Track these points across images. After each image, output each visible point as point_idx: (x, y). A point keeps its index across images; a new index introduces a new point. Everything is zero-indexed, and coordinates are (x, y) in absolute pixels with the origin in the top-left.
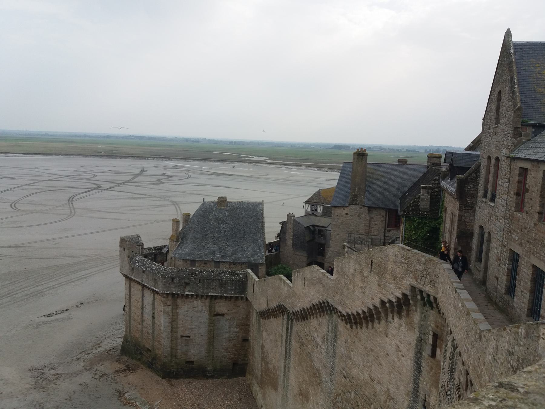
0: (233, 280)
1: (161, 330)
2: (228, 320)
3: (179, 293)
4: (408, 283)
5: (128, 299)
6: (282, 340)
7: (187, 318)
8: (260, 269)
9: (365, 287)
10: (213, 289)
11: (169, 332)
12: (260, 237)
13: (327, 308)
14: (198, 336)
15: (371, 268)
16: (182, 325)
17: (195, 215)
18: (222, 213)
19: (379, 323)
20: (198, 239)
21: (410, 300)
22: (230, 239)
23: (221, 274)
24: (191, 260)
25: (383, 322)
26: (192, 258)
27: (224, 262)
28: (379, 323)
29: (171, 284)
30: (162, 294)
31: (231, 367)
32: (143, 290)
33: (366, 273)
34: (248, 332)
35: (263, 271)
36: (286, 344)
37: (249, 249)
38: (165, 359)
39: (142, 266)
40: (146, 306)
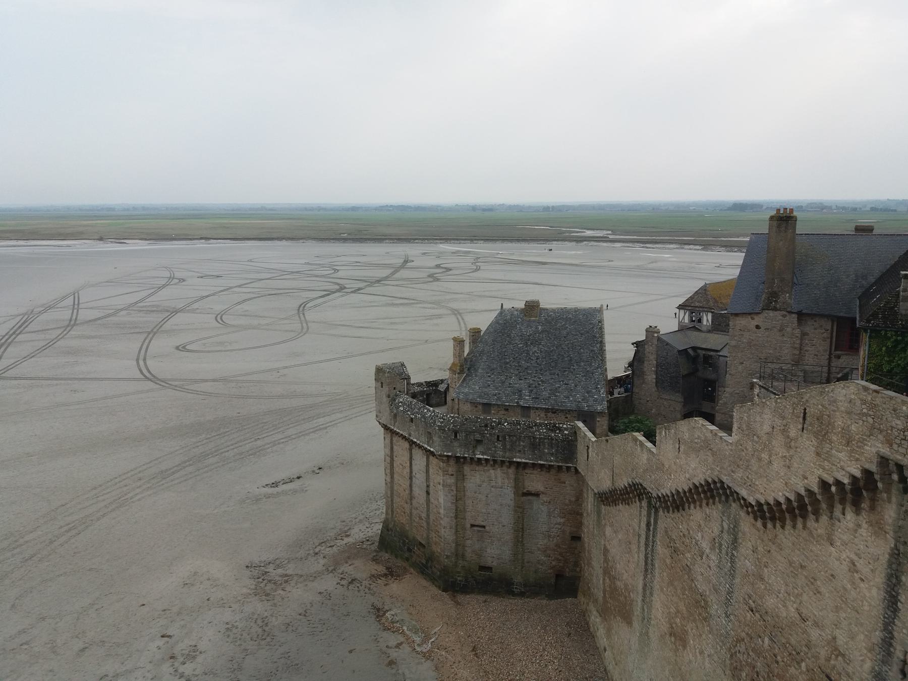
0: (552, 439)
1: (439, 513)
2: (547, 504)
3: (466, 455)
4: (874, 450)
5: (389, 462)
6: (639, 542)
7: (480, 496)
8: (598, 421)
9: (791, 457)
10: (520, 451)
11: (452, 517)
12: (597, 368)
13: (721, 492)
14: (497, 527)
15: (804, 423)
16: (473, 507)
17: (488, 331)
18: (531, 327)
19: (817, 520)
20: (493, 369)
21: (876, 481)
22: (546, 371)
23: (532, 428)
24: (484, 404)
25: (824, 519)
26: (485, 401)
27: (537, 409)
28: (817, 520)
29: (453, 441)
30: (440, 456)
31: (553, 581)
32: (411, 450)
33: (793, 433)
34: (580, 525)
35: (603, 425)
36: (646, 550)
37: (579, 388)
38: (446, 560)
39: (409, 411)
40: (416, 474)
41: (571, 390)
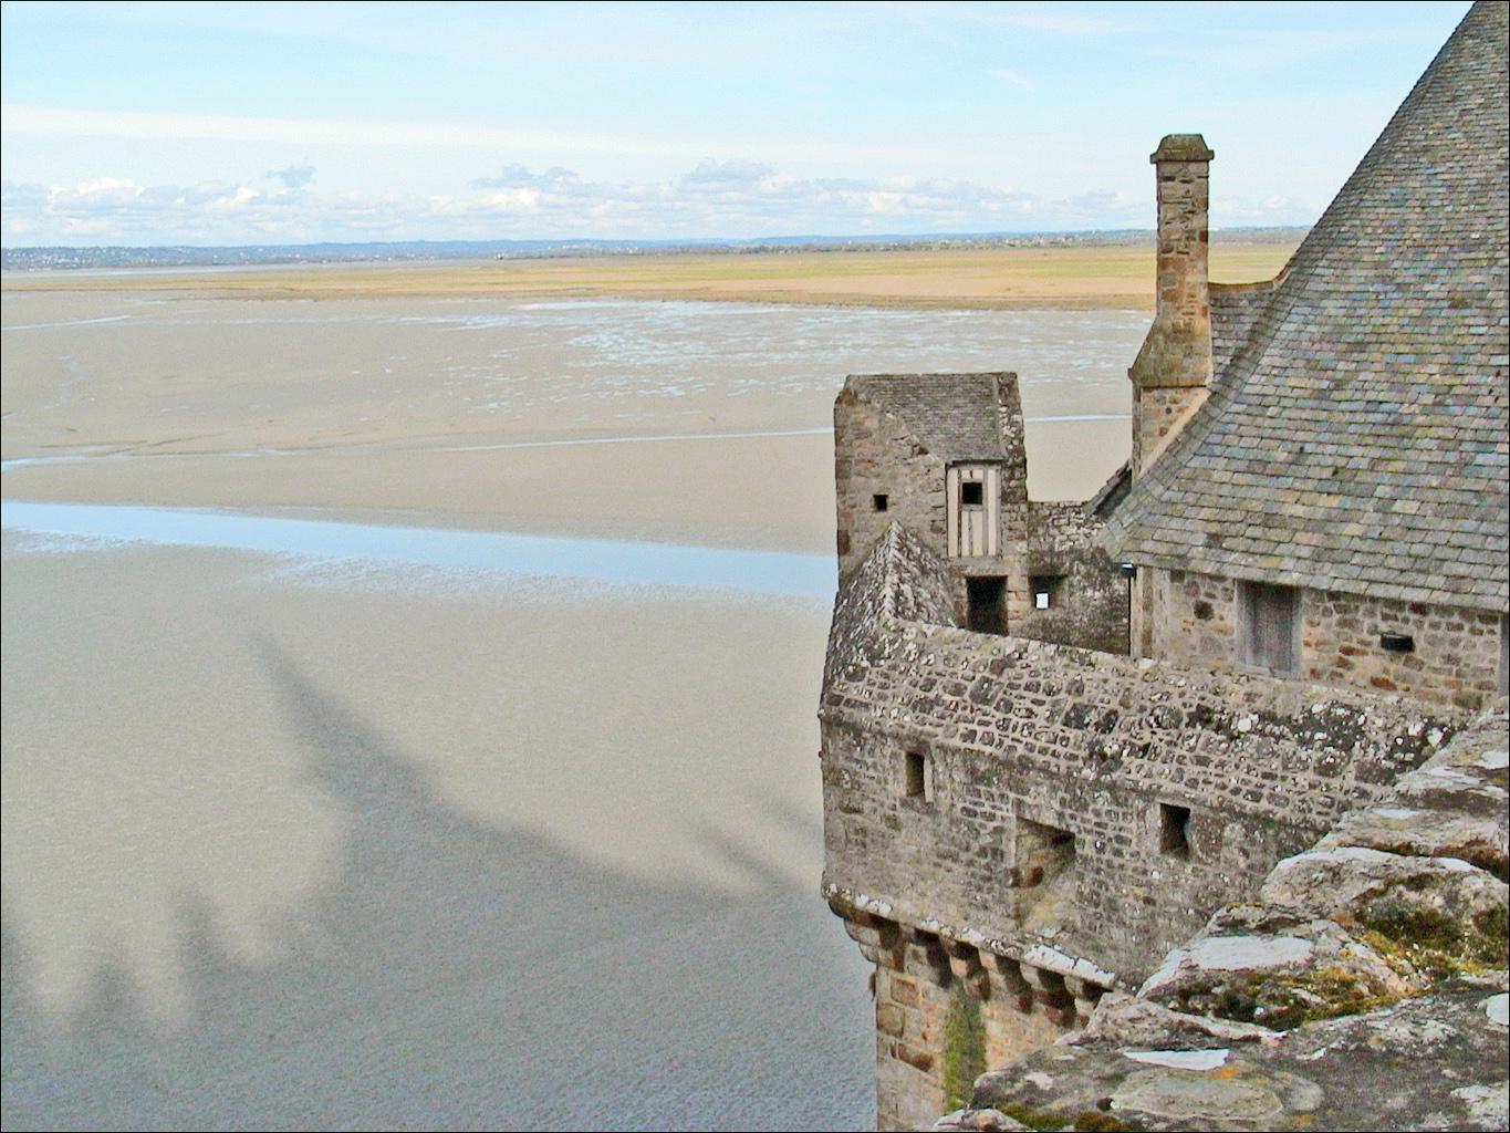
3: (974, 937)
20: (1360, 346)
29: (901, 814)
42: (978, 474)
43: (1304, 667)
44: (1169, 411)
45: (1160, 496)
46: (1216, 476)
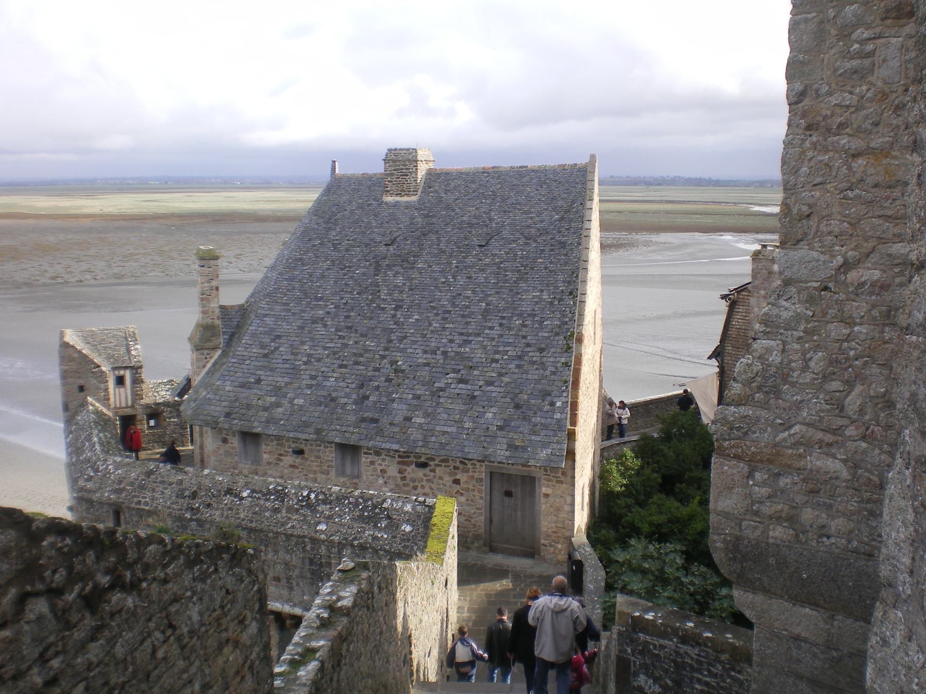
8: (547, 496)
20: (279, 337)
26: (237, 424)
35: (558, 510)
41: (474, 397)
42: (122, 372)
43: (264, 461)
44: (206, 358)
45: (206, 396)
46: (227, 388)
